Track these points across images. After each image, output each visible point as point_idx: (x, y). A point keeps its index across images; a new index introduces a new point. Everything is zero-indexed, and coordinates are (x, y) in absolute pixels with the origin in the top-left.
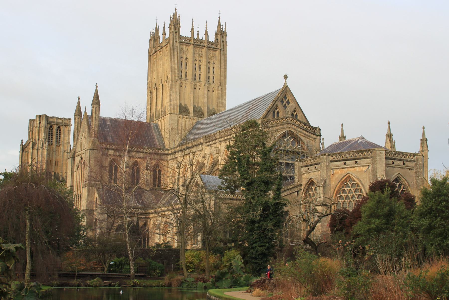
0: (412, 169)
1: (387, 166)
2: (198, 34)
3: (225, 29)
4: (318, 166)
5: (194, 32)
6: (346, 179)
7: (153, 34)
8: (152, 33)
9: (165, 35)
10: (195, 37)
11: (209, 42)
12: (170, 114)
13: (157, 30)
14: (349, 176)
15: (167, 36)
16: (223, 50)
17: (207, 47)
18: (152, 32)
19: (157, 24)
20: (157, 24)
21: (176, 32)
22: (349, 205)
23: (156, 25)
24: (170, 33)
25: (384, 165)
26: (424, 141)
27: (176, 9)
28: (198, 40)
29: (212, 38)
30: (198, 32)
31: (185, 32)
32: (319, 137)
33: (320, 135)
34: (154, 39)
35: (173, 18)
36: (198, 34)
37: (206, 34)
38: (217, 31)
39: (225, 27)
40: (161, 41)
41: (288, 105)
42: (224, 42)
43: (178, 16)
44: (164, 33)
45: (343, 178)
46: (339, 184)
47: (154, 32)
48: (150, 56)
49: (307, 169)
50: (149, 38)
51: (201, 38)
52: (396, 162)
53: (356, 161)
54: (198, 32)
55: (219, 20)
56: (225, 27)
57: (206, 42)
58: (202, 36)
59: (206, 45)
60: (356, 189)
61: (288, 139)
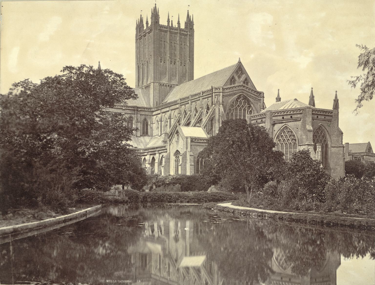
0: (330, 121)
1: (313, 119)
2: (172, 23)
3: (193, 19)
4: (263, 120)
5: (169, 22)
6: (283, 128)
7: (139, 23)
8: (138, 23)
9: (148, 24)
10: (170, 25)
11: (181, 30)
12: (154, 82)
13: (141, 20)
14: (286, 126)
15: (149, 25)
16: (192, 36)
17: (169, 31)
18: (138, 21)
19: (141, 15)
20: (141, 15)
21: (156, 22)
22: (294, 146)
23: (141, 17)
24: (152, 23)
25: (311, 119)
26: (336, 102)
27: (156, 4)
28: (172, 28)
29: (183, 26)
30: (172, 21)
31: (163, 21)
32: (262, 99)
33: (263, 97)
34: (139, 26)
35: (154, 11)
36: (172, 23)
37: (179, 23)
38: (187, 21)
39: (193, 18)
40: (145, 28)
41: (241, 76)
42: (192, 29)
43: (157, 9)
44: (147, 23)
45: (282, 127)
46: (279, 132)
47: (139, 21)
48: (137, 40)
49: (256, 122)
50: (135, 26)
51: (174, 26)
52: (319, 117)
53: (291, 115)
54: (172, 21)
55: (188, 13)
56: (193, 18)
57: (179, 29)
58: (175, 25)
59: (178, 31)
60: (291, 135)
61: (240, 101)
